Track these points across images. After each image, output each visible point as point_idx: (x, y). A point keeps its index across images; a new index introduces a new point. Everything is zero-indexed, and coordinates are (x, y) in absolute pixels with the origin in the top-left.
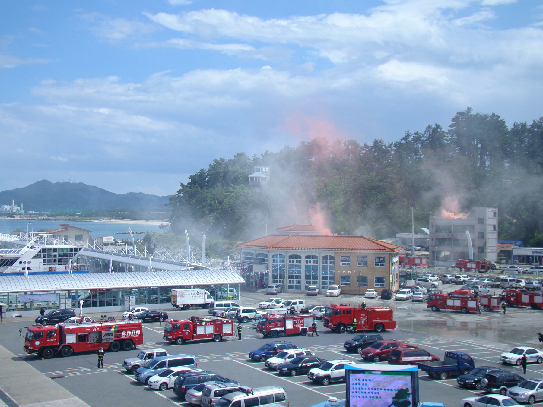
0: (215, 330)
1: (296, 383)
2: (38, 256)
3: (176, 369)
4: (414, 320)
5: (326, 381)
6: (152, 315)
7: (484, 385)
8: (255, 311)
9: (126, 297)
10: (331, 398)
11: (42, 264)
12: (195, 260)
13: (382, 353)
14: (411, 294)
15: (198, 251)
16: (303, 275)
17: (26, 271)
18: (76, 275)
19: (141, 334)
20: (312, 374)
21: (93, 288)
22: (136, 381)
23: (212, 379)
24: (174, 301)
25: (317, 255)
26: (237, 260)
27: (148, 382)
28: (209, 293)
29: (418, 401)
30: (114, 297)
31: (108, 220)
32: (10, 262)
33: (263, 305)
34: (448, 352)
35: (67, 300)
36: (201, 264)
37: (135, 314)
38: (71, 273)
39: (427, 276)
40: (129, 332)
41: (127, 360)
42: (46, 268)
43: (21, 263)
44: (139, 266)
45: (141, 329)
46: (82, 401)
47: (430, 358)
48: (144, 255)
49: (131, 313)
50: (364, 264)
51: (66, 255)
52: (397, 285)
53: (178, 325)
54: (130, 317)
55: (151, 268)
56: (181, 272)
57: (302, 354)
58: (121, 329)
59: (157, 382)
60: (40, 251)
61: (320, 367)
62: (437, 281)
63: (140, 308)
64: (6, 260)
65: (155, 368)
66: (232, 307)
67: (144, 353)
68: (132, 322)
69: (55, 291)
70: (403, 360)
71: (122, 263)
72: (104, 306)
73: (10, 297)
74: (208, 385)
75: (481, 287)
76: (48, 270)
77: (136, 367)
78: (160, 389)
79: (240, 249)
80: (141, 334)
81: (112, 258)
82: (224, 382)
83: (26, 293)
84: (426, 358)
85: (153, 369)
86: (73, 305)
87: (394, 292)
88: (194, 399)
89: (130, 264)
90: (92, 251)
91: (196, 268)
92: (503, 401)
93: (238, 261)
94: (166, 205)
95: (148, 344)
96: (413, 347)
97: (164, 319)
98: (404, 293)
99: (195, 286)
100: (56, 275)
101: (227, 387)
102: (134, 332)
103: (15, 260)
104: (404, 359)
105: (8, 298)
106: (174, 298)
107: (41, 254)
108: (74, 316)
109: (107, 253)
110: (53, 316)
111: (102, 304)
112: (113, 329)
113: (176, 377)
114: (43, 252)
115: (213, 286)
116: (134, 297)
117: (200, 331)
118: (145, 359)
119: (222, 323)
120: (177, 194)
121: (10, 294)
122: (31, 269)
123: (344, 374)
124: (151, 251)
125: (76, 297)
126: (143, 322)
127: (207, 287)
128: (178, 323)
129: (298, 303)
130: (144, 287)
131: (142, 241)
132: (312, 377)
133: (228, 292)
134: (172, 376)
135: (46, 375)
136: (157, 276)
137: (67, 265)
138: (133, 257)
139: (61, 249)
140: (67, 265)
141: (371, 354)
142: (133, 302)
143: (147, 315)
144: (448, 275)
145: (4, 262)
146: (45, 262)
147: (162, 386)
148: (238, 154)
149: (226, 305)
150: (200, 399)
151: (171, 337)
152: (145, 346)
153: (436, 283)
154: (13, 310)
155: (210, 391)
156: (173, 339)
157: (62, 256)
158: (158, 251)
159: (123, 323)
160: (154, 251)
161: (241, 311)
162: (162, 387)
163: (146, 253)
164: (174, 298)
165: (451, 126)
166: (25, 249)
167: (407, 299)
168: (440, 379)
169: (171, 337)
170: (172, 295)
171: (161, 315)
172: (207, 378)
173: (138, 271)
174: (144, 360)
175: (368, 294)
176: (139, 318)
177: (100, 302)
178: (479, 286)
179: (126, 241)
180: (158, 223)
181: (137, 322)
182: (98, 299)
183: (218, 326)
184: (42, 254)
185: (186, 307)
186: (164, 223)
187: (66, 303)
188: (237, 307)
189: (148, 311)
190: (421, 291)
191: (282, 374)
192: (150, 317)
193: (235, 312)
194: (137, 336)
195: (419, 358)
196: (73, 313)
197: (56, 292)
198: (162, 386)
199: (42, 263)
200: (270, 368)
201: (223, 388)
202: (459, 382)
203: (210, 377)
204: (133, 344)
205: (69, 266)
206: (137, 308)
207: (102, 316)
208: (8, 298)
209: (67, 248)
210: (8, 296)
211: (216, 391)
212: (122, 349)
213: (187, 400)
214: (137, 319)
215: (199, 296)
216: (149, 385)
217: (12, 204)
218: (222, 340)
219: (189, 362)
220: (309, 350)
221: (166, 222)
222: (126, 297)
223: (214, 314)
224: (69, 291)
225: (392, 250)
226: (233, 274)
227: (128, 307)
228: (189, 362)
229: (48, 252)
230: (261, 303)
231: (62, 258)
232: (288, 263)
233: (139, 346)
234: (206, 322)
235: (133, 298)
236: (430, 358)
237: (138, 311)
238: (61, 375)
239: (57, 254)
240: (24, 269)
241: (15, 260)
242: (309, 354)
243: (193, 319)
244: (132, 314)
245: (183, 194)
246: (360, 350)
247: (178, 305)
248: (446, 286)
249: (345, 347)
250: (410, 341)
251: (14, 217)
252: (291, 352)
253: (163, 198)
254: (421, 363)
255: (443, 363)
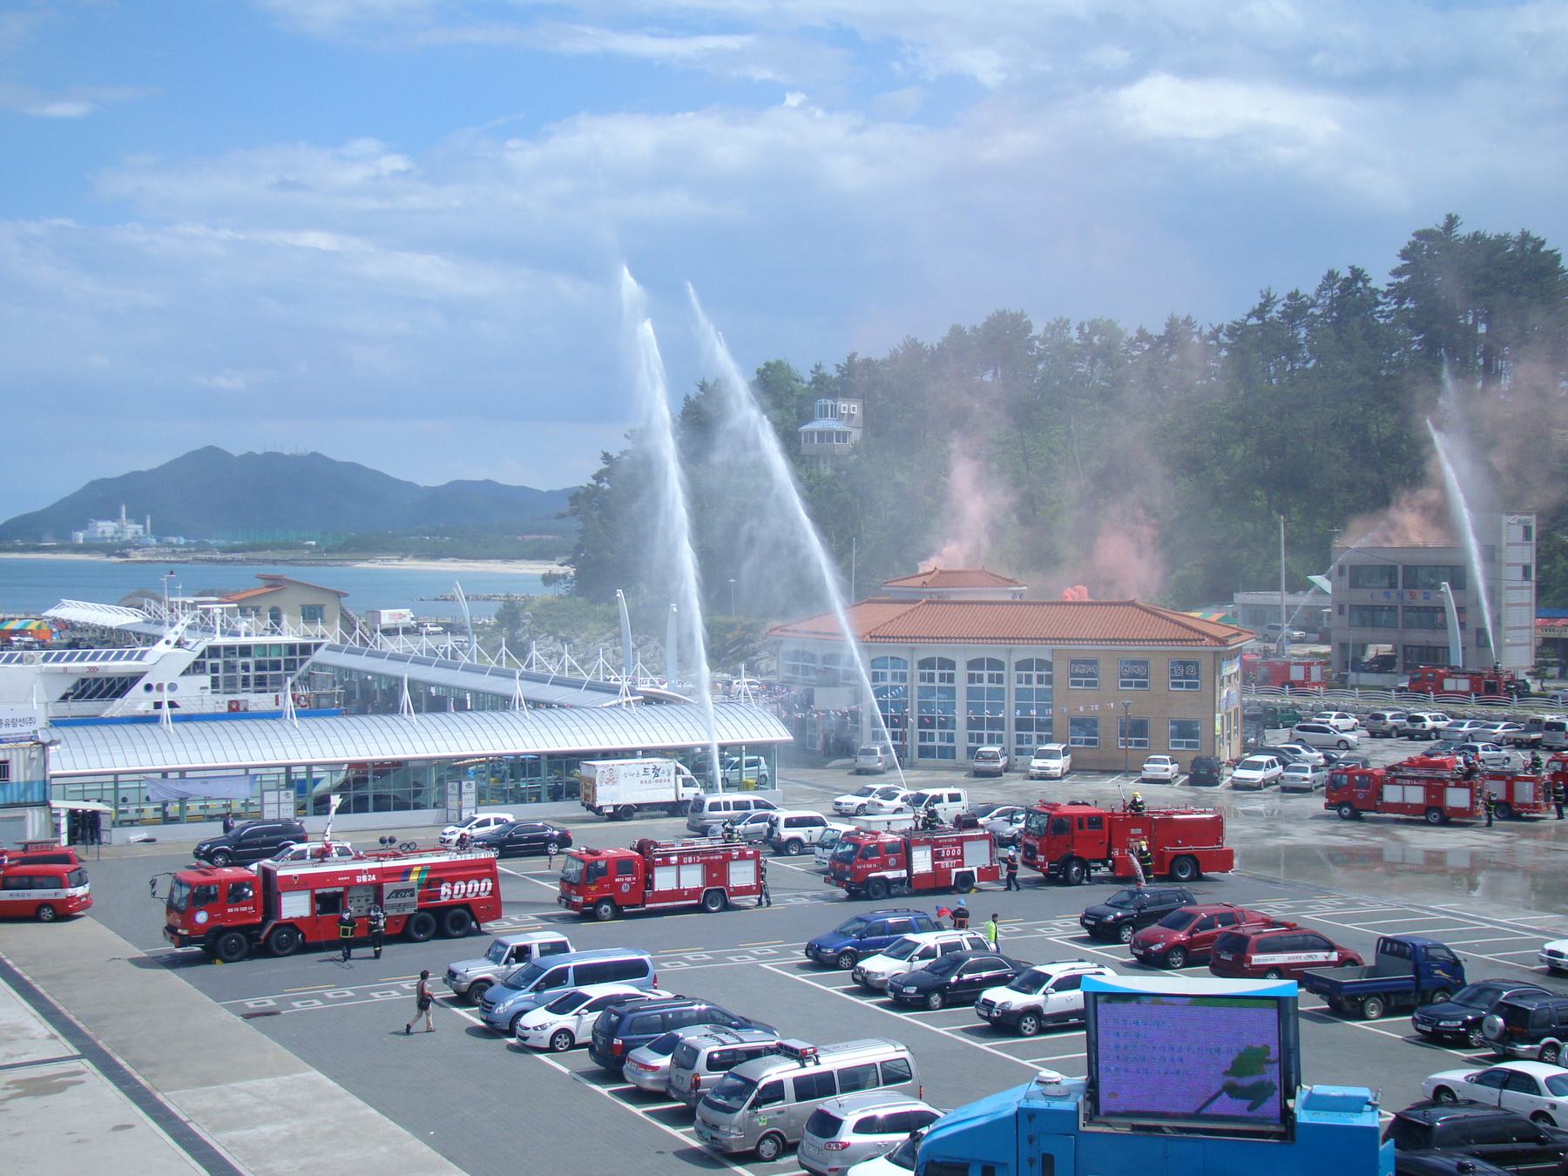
0: (708, 879)
1: (941, 1030)
2: (196, 668)
3: (597, 991)
4: (1287, 847)
5: (1029, 1024)
6: (525, 836)
7: (1492, 1035)
8: (823, 824)
9: (450, 784)
10: (1046, 1074)
11: (210, 690)
12: (646, 675)
13: (1192, 942)
14: (1279, 769)
15: (656, 648)
16: (961, 716)
17: (166, 711)
18: (307, 720)
19: (495, 892)
20: (989, 1004)
21: (355, 758)
22: (481, 1024)
23: (701, 1019)
24: (587, 796)
25: (904, 655)
26: (768, 673)
27: (518, 1027)
28: (688, 773)
29: (1299, 1083)
30: (415, 783)
31: (395, 562)
32: (118, 687)
33: (843, 806)
34: (1387, 940)
35: (282, 793)
36: (666, 686)
37: (477, 832)
38: (291, 716)
39: (1324, 716)
40: (460, 886)
41: (458, 967)
42: (219, 703)
43: (148, 687)
44: (486, 694)
45: (494, 876)
46: (330, 1083)
47: (1334, 956)
48: (499, 662)
49: (465, 830)
50: (1087, 683)
51: (276, 665)
52: (1236, 742)
53: (602, 864)
54: (463, 842)
55: (520, 700)
56: (606, 710)
57: (958, 946)
58: (437, 875)
59: (543, 1027)
60: (202, 655)
61: (1013, 983)
62: (1353, 730)
63: (492, 816)
64: (108, 680)
65: (537, 989)
66: (754, 812)
67: (506, 946)
68: (469, 857)
69: (247, 768)
70: (1253, 963)
71: (437, 685)
72: (389, 810)
73: (120, 786)
74: (691, 1035)
75: (1485, 749)
76: (225, 709)
77: (484, 984)
78: (552, 1049)
79: (775, 643)
80: (495, 892)
81: (407, 671)
82: (736, 1028)
83: (165, 774)
84: (1320, 956)
85: (531, 991)
86: (301, 809)
87: (1228, 765)
88: (650, 1077)
89: (464, 690)
90: (351, 651)
91: (651, 700)
92: (1549, 1081)
93: (773, 678)
94: (561, 516)
95: (516, 919)
96: (1283, 924)
97: (561, 846)
98: (1256, 766)
99: (647, 752)
100: (248, 722)
101: (742, 1041)
102: (474, 885)
103: (134, 679)
104: (1258, 959)
105: (116, 789)
106: (588, 787)
107: (204, 663)
108: (302, 840)
109: (394, 657)
110: (243, 841)
111: (382, 804)
112: (414, 877)
113: (597, 1015)
114: (210, 657)
115: (699, 750)
116: (473, 783)
117: (664, 880)
118: (507, 962)
119: (728, 858)
120: (592, 486)
121: (121, 778)
122: (178, 707)
123: (1080, 1005)
124: (520, 651)
125: (309, 784)
126: (502, 856)
127: (682, 754)
128: (602, 859)
129: (946, 798)
130: (500, 756)
131: (493, 621)
132: (989, 1012)
133: (744, 769)
134: (586, 1011)
135: (226, 1007)
136: (538, 724)
137: (281, 695)
138: (467, 668)
139: (262, 647)
140: (281, 695)
141: (1160, 946)
142: (470, 798)
143: (510, 836)
144: (1388, 714)
145: (100, 687)
146: (218, 687)
147: (558, 1039)
148: (768, 365)
149: (739, 806)
150: (666, 1077)
151: (580, 899)
152: (507, 924)
153: (1351, 737)
154: (132, 823)
155: (695, 1053)
156: (585, 904)
157: (265, 669)
158: (538, 650)
159: (444, 859)
160: (529, 650)
161: (782, 823)
162: (558, 1043)
163: (504, 657)
164: (588, 787)
165: (1397, 273)
166: (160, 648)
167: (1266, 783)
168: (1362, 1016)
169: (580, 899)
170: (581, 778)
171: (552, 835)
172: (686, 1015)
173: (483, 709)
174: (505, 966)
175: (1151, 770)
176: (488, 843)
177: (376, 798)
178: (1480, 745)
179: (449, 620)
180: (538, 568)
181: (484, 855)
182: (370, 790)
183: (716, 868)
184: (209, 662)
185: (623, 813)
186: (555, 568)
187: (279, 803)
188: (771, 812)
189: (513, 825)
190: (1307, 761)
191: (901, 1004)
192: (520, 840)
193: (764, 826)
194: (484, 895)
195: (1302, 957)
196: (301, 830)
197: (252, 772)
198: (558, 1039)
199: (209, 686)
200: (868, 987)
201: (732, 1043)
202: (1419, 1026)
203: (694, 1015)
204: (474, 919)
205: (285, 696)
206: (481, 817)
207: (382, 841)
208: (116, 789)
209: (280, 645)
210: (116, 782)
211: (711, 1054)
212: (442, 934)
213: (629, 1080)
214: (481, 847)
215: (661, 781)
216: (519, 1036)
217: (119, 517)
218: (727, 907)
219: (633, 970)
220: (981, 936)
221: (562, 565)
222: (450, 784)
223: (704, 831)
224: (288, 767)
225: (1223, 642)
226: (758, 715)
227: (456, 813)
228: (633, 970)
229: (225, 656)
230: (838, 799)
231: (265, 673)
232: (918, 683)
233: (490, 926)
234: (681, 855)
235: (470, 788)
236: (1334, 956)
237: (485, 823)
238: (271, 1007)
239: (250, 661)
240: (158, 705)
241: (134, 679)
242: (978, 945)
243: (643, 847)
244: (468, 832)
245: (608, 482)
246: (1127, 934)
247: (601, 807)
248: (1380, 744)
249: (1082, 923)
250: (1276, 909)
251: (126, 556)
252: (928, 939)
253: (551, 494)
254: (1307, 971)
255: (1372, 971)
